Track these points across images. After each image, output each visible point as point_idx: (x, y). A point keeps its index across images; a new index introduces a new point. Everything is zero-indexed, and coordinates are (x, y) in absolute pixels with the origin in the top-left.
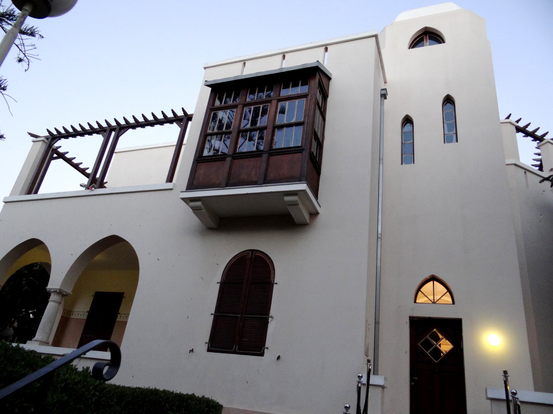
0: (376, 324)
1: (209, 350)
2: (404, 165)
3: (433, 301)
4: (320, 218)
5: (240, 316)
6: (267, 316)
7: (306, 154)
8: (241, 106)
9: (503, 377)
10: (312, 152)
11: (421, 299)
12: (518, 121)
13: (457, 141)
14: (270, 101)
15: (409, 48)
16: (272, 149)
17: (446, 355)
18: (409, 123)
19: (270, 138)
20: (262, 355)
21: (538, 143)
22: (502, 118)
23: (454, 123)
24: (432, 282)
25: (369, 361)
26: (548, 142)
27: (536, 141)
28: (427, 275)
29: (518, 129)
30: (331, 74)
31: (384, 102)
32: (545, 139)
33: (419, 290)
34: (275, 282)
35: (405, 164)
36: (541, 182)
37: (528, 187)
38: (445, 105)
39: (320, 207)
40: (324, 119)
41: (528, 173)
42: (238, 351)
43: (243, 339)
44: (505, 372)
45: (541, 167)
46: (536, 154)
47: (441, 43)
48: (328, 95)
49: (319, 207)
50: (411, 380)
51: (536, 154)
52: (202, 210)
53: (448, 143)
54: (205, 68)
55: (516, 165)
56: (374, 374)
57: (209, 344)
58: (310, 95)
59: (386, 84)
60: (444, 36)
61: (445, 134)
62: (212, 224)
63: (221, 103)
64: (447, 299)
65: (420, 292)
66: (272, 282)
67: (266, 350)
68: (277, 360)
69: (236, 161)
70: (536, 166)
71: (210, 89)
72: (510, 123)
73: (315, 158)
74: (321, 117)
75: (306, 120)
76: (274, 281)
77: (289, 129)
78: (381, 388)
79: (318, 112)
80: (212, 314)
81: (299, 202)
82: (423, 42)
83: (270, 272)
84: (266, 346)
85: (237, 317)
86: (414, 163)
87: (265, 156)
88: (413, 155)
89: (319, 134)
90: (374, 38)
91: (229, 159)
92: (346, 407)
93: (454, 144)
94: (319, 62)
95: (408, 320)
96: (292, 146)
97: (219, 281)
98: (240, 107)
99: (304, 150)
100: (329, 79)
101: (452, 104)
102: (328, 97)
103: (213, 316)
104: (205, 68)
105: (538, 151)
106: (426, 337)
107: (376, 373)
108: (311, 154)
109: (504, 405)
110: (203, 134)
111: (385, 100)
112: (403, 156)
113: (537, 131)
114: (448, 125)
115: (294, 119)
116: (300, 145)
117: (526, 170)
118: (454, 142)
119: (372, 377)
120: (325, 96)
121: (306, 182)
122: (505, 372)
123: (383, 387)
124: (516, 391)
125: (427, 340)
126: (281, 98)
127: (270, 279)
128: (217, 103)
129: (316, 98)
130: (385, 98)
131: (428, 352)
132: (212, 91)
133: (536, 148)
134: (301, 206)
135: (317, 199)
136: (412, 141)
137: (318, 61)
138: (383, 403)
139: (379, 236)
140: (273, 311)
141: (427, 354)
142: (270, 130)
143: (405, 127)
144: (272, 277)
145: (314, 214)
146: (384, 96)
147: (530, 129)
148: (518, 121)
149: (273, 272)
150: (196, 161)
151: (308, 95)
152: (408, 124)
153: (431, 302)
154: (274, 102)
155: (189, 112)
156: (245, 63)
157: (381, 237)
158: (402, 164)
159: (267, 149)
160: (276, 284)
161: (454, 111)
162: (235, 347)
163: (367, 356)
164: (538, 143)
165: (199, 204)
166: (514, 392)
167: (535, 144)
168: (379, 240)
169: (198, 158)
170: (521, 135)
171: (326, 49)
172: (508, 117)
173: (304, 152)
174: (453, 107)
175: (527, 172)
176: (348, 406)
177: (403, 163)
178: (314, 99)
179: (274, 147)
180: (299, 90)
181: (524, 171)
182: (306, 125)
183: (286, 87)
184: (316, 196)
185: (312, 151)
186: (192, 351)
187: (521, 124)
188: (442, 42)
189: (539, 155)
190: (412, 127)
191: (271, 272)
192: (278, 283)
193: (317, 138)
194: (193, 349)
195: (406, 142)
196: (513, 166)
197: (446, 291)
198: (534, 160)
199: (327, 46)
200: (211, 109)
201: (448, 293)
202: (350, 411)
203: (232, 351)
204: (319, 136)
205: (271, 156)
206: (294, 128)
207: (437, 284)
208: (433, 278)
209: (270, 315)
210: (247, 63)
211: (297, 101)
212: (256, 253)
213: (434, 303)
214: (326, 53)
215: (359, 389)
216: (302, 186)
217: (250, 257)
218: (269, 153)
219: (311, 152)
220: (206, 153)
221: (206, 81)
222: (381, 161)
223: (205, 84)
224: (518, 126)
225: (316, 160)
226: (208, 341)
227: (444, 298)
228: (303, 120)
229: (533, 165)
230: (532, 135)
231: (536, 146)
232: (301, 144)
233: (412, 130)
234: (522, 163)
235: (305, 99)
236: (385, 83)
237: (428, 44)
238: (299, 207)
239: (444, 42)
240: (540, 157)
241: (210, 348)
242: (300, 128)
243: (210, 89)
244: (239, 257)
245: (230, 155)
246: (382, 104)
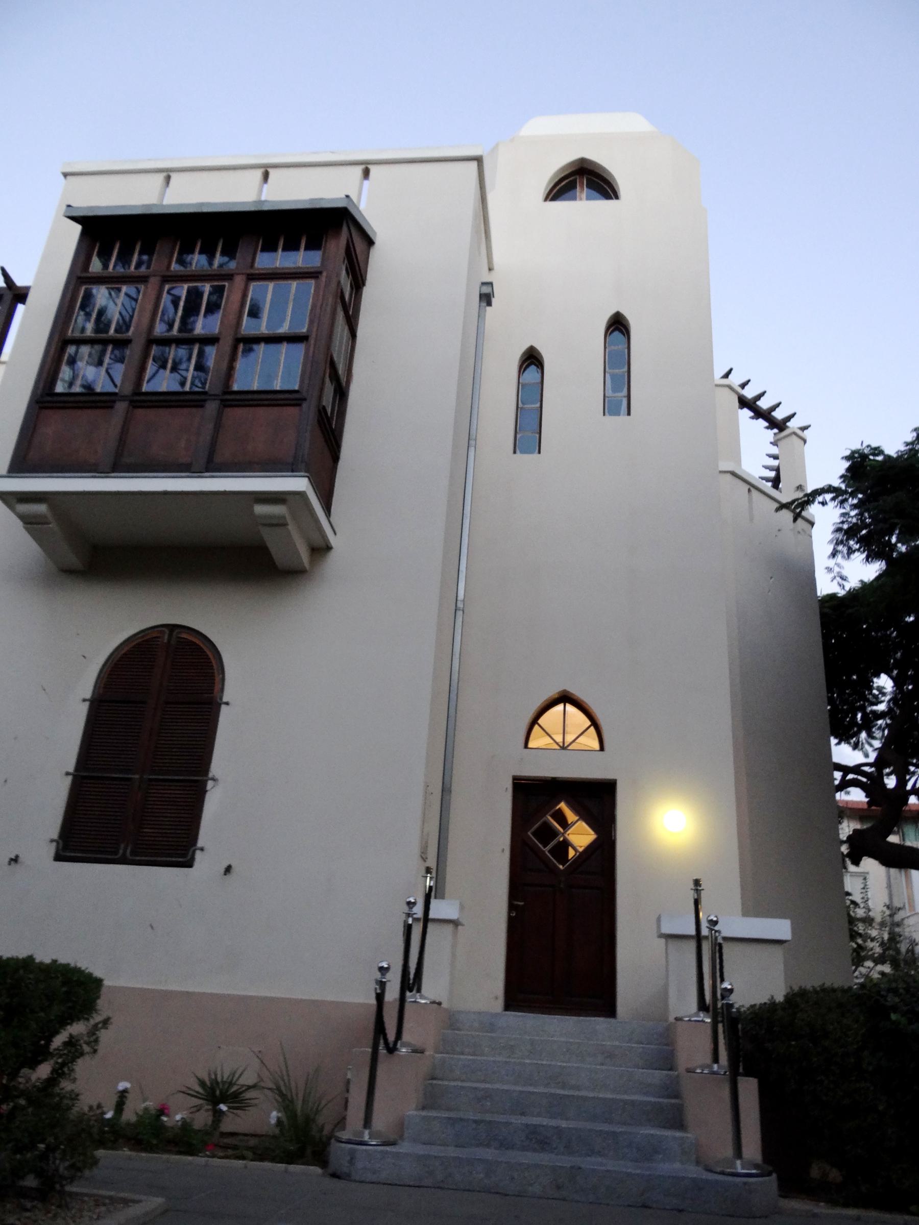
0: (444, 793)
1: (58, 858)
2: (518, 455)
3: (561, 744)
4: (333, 556)
5: (137, 776)
6: (202, 776)
7: (309, 409)
8: (158, 278)
9: (693, 891)
10: (324, 408)
11: (538, 741)
12: (743, 386)
13: (629, 414)
14: (230, 277)
15: (546, 200)
16: (229, 390)
17: (582, 854)
18: (535, 365)
19: (224, 365)
20: (189, 864)
21: (775, 434)
22: (719, 372)
23: (626, 374)
24: (560, 707)
25: (428, 870)
26: (795, 433)
27: (772, 429)
28: (552, 692)
29: (744, 403)
30: (375, 233)
31: (486, 311)
32: (787, 427)
33: (534, 721)
34: (225, 700)
35: (523, 452)
36: (777, 510)
37: (751, 520)
38: (610, 334)
39: (335, 534)
40: (353, 335)
41: (753, 491)
42: (131, 858)
43: (145, 830)
44: (697, 883)
45: (776, 482)
46: (770, 456)
47: (610, 198)
48: (366, 279)
49: (332, 532)
50: (511, 907)
51: (770, 456)
52: (48, 523)
53: (610, 415)
54: (66, 175)
55: (734, 474)
56: (435, 898)
57: (58, 843)
58: (324, 274)
59: (493, 272)
60: (617, 184)
61: (606, 395)
62: (73, 560)
63: (105, 266)
64: (591, 741)
65: (536, 727)
66: (218, 700)
67: (198, 853)
68: (225, 874)
69: (140, 412)
70: (767, 479)
71: (78, 228)
72: (730, 387)
73: (329, 420)
74: (346, 328)
75: (315, 329)
76: (221, 698)
77: (272, 347)
78: (450, 927)
79: (340, 315)
80: (68, 774)
81: (289, 520)
82: (574, 191)
83: (212, 677)
84: (200, 844)
86: (539, 452)
87: (212, 407)
88: (538, 436)
89: (341, 366)
90: (474, 165)
91: (121, 407)
92: (381, 969)
93: (623, 418)
94: (351, 200)
95: (509, 785)
96: (278, 388)
97: (88, 695)
98: (154, 281)
99: (305, 399)
100: (370, 242)
101: (624, 335)
102: (364, 284)
103: (70, 778)
104: (66, 175)
105: (774, 450)
106: (544, 819)
107: (441, 895)
108: (322, 411)
109: (692, 945)
110: (56, 339)
111: (488, 308)
112: (518, 436)
113: (777, 409)
114: (613, 377)
115: (285, 324)
116: (296, 388)
117: (752, 486)
118: (624, 415)
119: (434, 903)
120: (358, 281)
121: (306, 474)
122: (697, 883)
123: (455, 923)
124: (716, 917)
125: (547, 825)
126: (257, 272)
127: (213, 693)
128: (96, 265)
129: (339, 282)
130: (489, 304)
131: (546, 850)
132: (83, 234)
133: (771, 443)
134: (291, 527)
135: (330, 515)
136: (538, 405)
137: (347, 196)
138: (454, 955)
139: (460, 605)
140: (217, 766)
141: (544, 852)
142: (226, 344)
143: (526, 372)
144: (217, 687)
145: (321, 549)
146: (486, 299)
147: (764, 404)
148: (743, 386)
149: (221, 676)
150: (37, 402)
151: (321, 273)
152: (533, 368)
153: (558, 748)
154: (239, 280)
155: (20, 282)
156: (168, 179)
157: (463, 607)
158: (515, 452)
159: (218, 390)
160: (227, 704)
161: (626, 350)
163: (424, 860)
164: (775, 434)
165: (41, 508)
166: (712, 920)
167: (771, 434)
168: (460, 613)
169: (42, 396)
170: (746, 413)
171: (366, 173)
172: (726, 376)
173: (305, 405)
174: (625, 340)
175: (752, 489)
176: (386, 966)
177: (518, 451)
178: (333, 285)
179: (235, 388)
180: (300, 259)
181: (747, 487)
182: (312, 341)
183: (270, 247)
184: (327, 508)
185: (324, 404)
186: (15, 860)
187: (749, 393)
188: (613, 196)
189: (776, 457)
190: (539, 376)
191: (214, 676)
193: (335, 376)
194: (17, 857)
195: (526, 406)
196: (729, 476)
197: (588, 723)
198: (766, 467)
199: (370, 166)
200: (79, 278)
201: (592, 728)
202: (388, 976)
203: (116, 857)
204: (340, 372)
205: (225, 406)
206: (284, 347)
207: (570, 708)
208: (565, 698)
209: (210, 775)
210: (174, 176)
211: (294, 284)
212: (180, 633)
213: (563, 748)
214: (366, 183)
215: (408, 929)
216: (298, 484)
217: (166, 641)
218: (222, 400)
219: (321, 408)
220: (60, 388)
221: (69, 206)
222: (472, 442)
223: (66, 211)
224: (743, 396)
225: (330, 425)
227: (581, 740)
228: (308, 330)
229: (763, 478)
231: (772, 440)
232: (300, 386)
233: (539, 380)
234: (745, 472)
235: (313, 282)
236: (490, 269)
237: (584, 195)
238: (289, 533)
239: (617, 197)
240: (775, 463)
241: (62, 853)
242: (299, 350)
243: (78, 228)
244: (140, 640)
245: (127, 396)
246: (481, 316)
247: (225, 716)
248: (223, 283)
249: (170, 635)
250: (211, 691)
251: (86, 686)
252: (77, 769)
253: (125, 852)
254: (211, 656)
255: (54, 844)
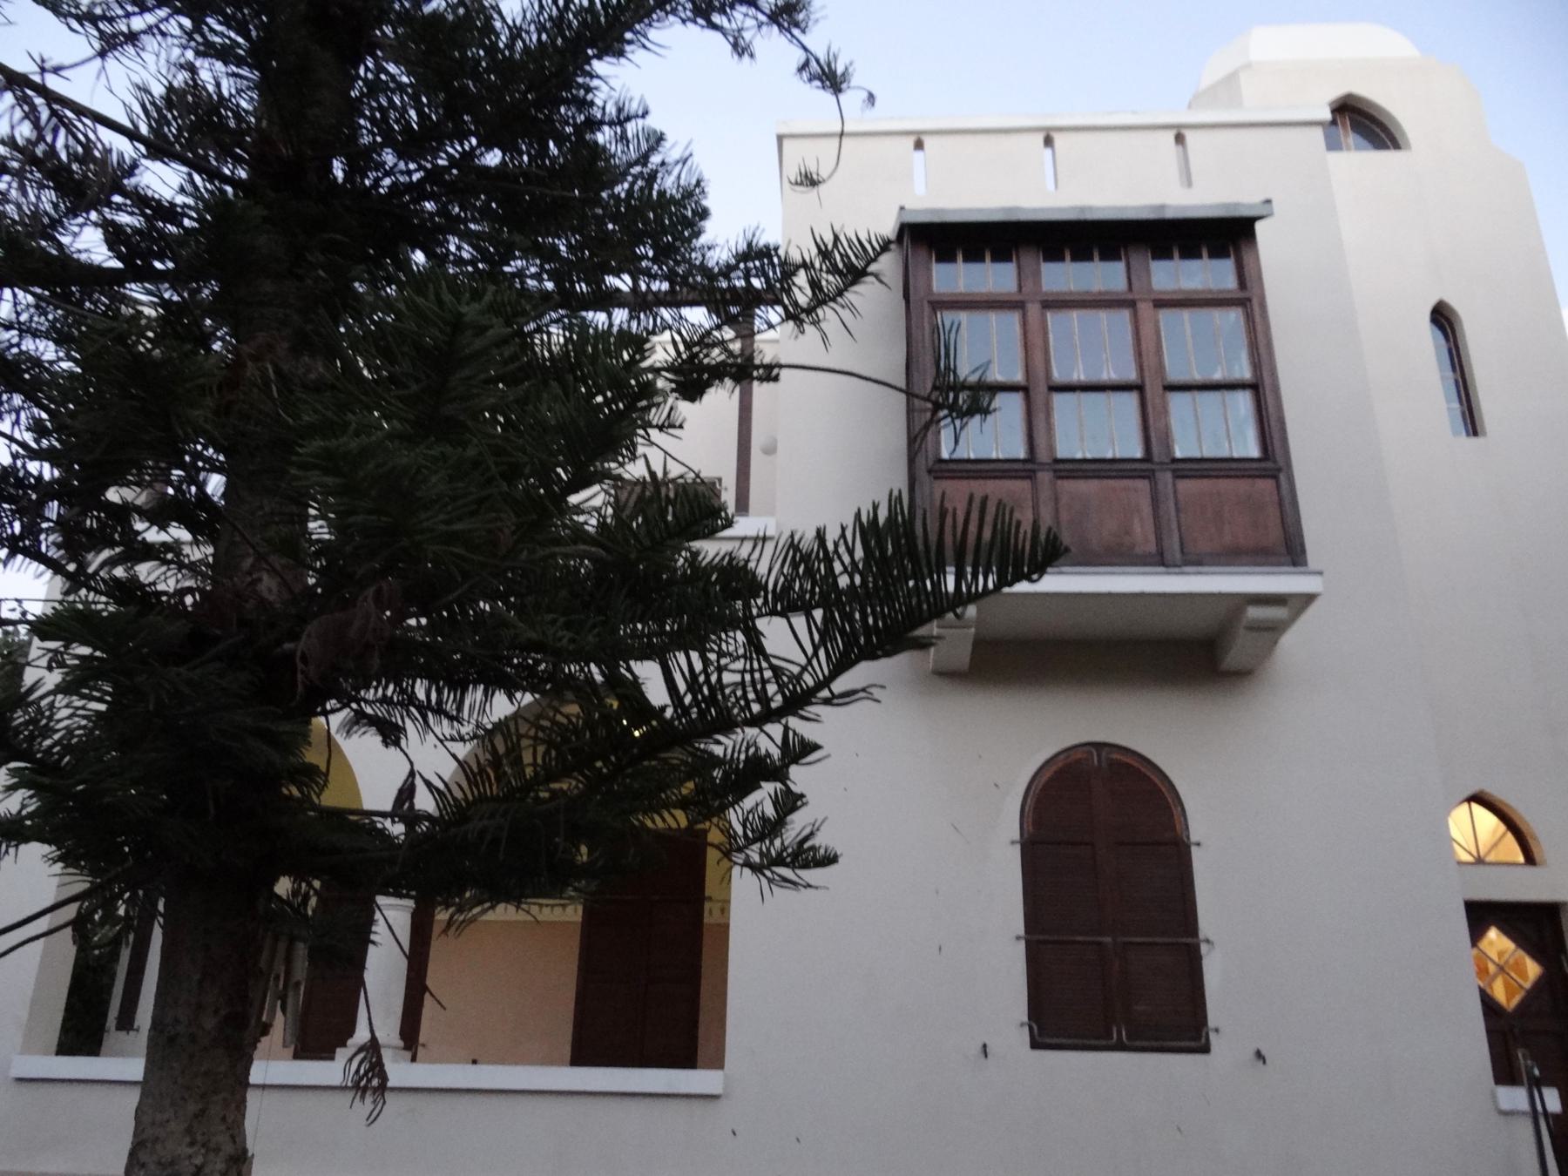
66: (1186, 840)
85: (1100, 944)
140: (1207, 922)
149: (1179, 809)
162: (1120, 1032)
192: (1202, 841)
209: (1202, 935)
226: (1025, 1019)
247: (1200, 862)
249: (1099, 756)
250: (1174, 828)
251: (1010, 826)
252: (1027, 932)
253: (1119, 1033)
254: (1157, 781)
255: (1026, 1029)
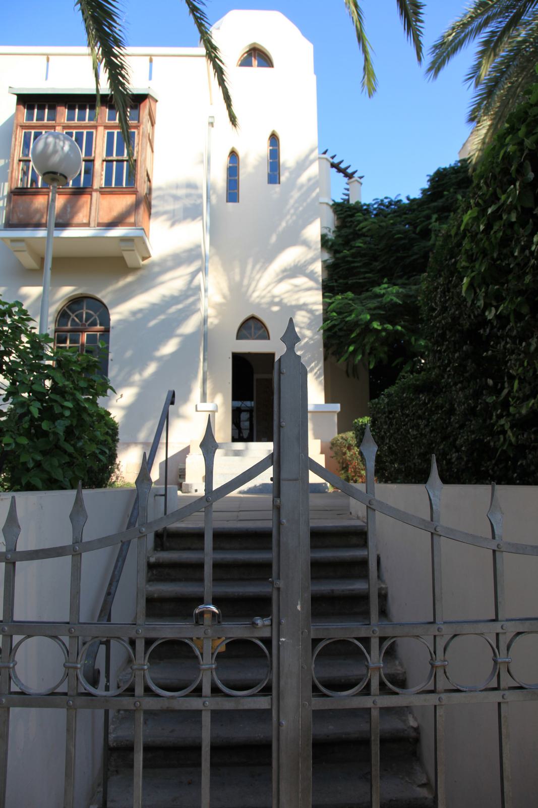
12: (333, 157)
26: (357, 181)
32: (354, 177)
47: (270, 67)
95: (231, 356)
102: (155, 123)
105: (348, 187)
111: (212, 128)
130: (213, 126)
147: (343, 166)
148: (333, 157)
167: (346, 179)
170: (334, 170)
172: (325, 153)
189: (348, 190)
223: (9, 90)
230: (343, 171)
236: (211, 104)
243: (15, 97)
248: (92, 130)
